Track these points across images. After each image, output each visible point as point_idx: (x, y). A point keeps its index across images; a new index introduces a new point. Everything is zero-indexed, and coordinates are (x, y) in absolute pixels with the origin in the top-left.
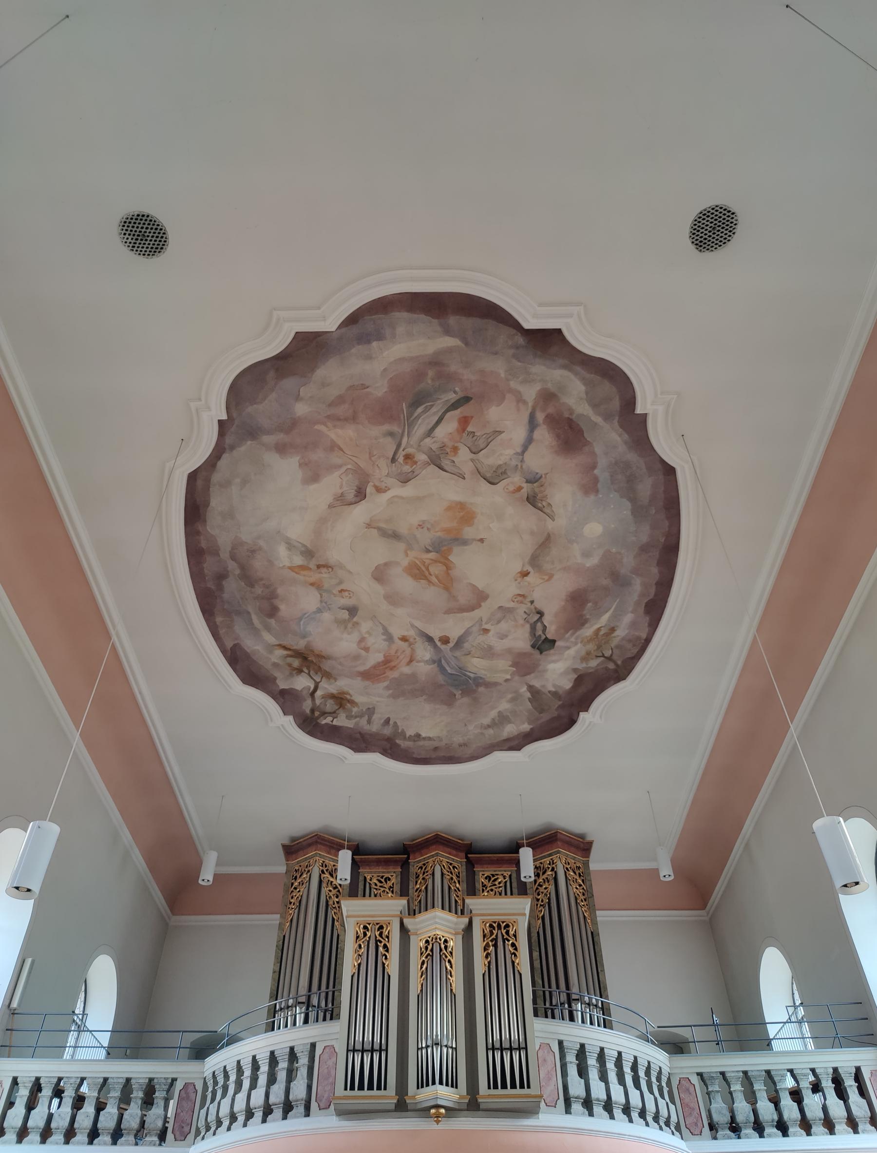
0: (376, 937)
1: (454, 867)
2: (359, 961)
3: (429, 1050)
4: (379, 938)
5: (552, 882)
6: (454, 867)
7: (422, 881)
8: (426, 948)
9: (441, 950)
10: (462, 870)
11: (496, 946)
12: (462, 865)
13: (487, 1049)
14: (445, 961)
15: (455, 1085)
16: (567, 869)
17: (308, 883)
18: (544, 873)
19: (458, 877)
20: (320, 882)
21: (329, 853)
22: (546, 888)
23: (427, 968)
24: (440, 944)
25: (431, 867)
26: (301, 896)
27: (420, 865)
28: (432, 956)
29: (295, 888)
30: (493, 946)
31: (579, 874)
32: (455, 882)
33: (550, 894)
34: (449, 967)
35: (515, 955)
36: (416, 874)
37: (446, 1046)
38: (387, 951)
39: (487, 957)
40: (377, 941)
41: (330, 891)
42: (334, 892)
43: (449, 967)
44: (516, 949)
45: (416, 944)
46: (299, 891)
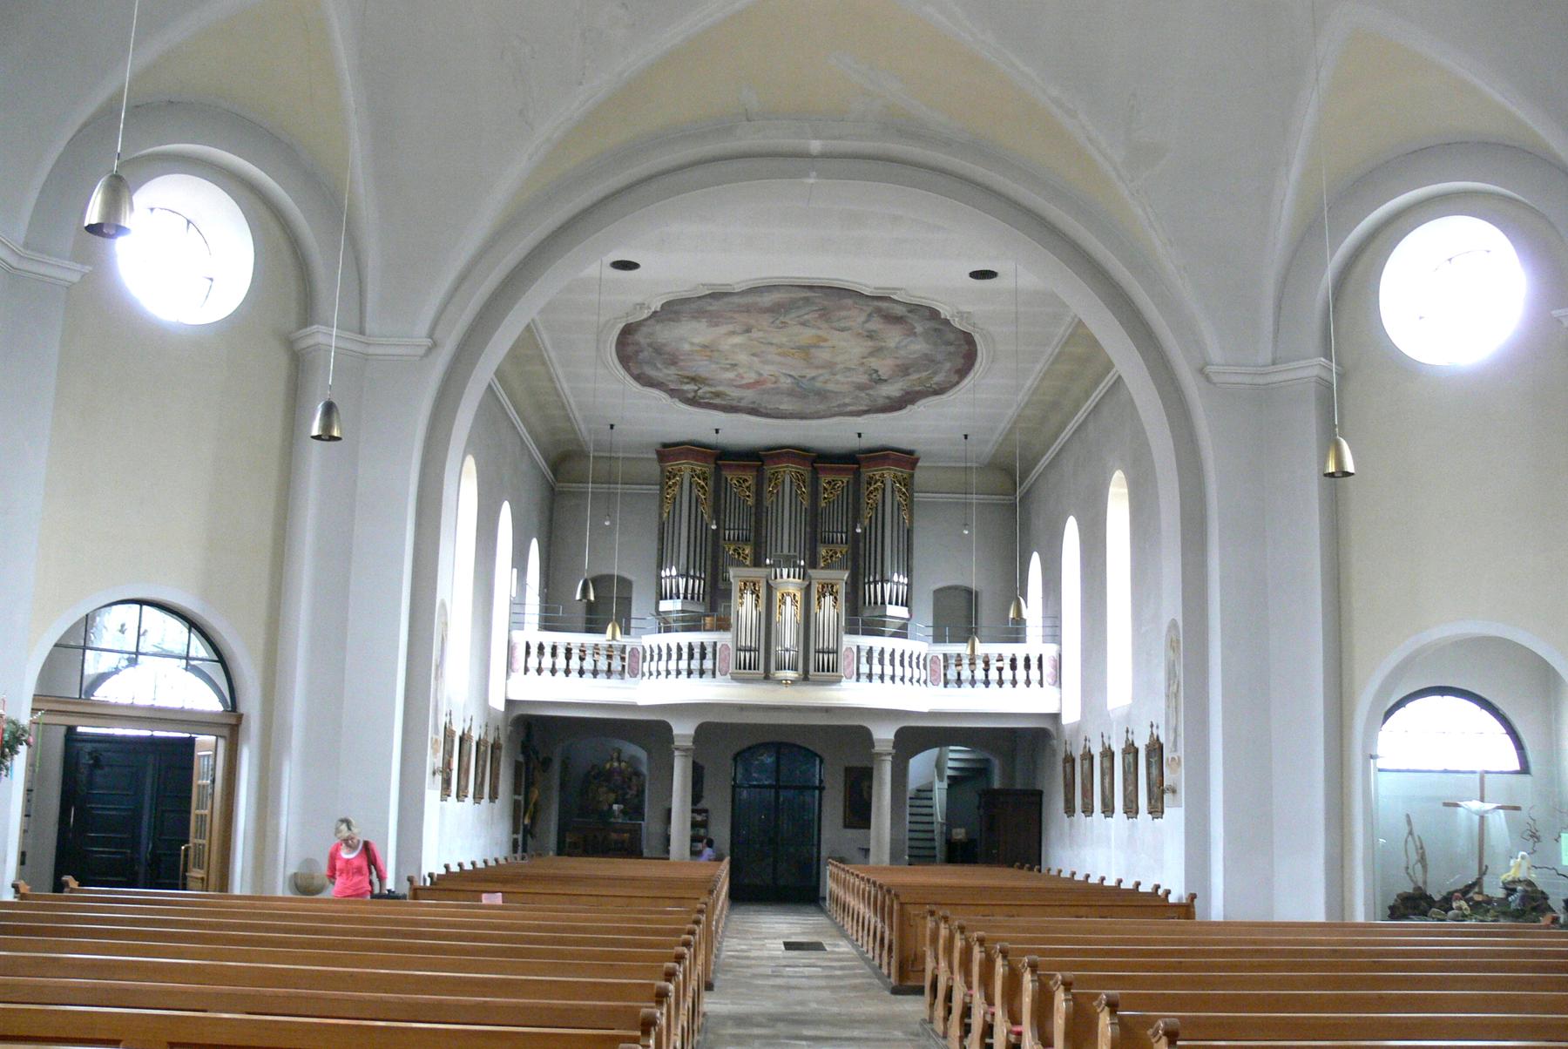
5: (880, 491)
10: (808, 476)
15: (796, 670)
18: (875, 484)
19: (804, 482)
20: (691, 483)
27: (772, 471)
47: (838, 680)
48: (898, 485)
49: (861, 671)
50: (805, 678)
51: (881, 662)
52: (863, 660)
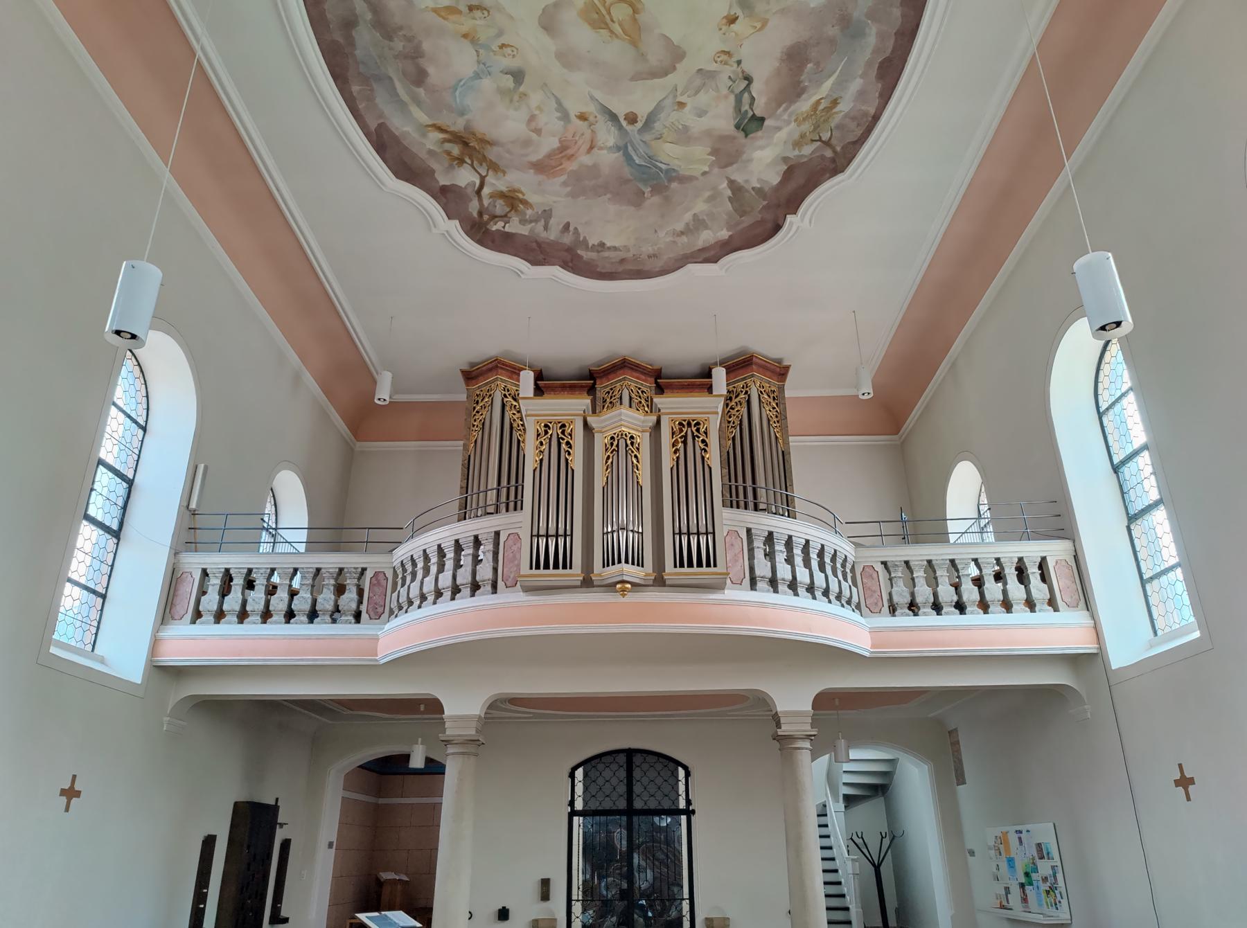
0: (558, 435)
1: (642, 392)
2: (541, 457)
3: (615, 535)
4: (561, 435)
5: (745, 405)
6: (642, 392)
7: (610, 405)
8: (612, 444)
9: (627, 446)
11: (685, 443)
12: (651, 391)
13: (674, 534)
14: (632, 456)
16: (761, 392)
17: (490, 408)
18: (736, 397)
20: (503, 406)
21: (510, 378)
22: (738, 411)
23: (612, 463)
24: (626, 440)
25: (619, 391)
26: (484, 419)
27: (607, 390)
28: (618, 451)
29: (478, 412)
30: (682, 442)
31: (774, 397)
32: (643, 406)
33: (742, 416)
34: (635, 462)
35: (706, 451)
36: (603, 398)
37: (632, 531)
38: (571, 447)
39: (675, 452)
40: (559, 439)
41: (514, 414)
42: (518, 415)
43: (635, 462)
44: (706, 445)
45: (600, 441)
46: (482, 414)
47: (719, 587)
48: (766, 397)
49: (758, 572)
50: (660, 581)
51: (790, 560)
52: (759, 555)
